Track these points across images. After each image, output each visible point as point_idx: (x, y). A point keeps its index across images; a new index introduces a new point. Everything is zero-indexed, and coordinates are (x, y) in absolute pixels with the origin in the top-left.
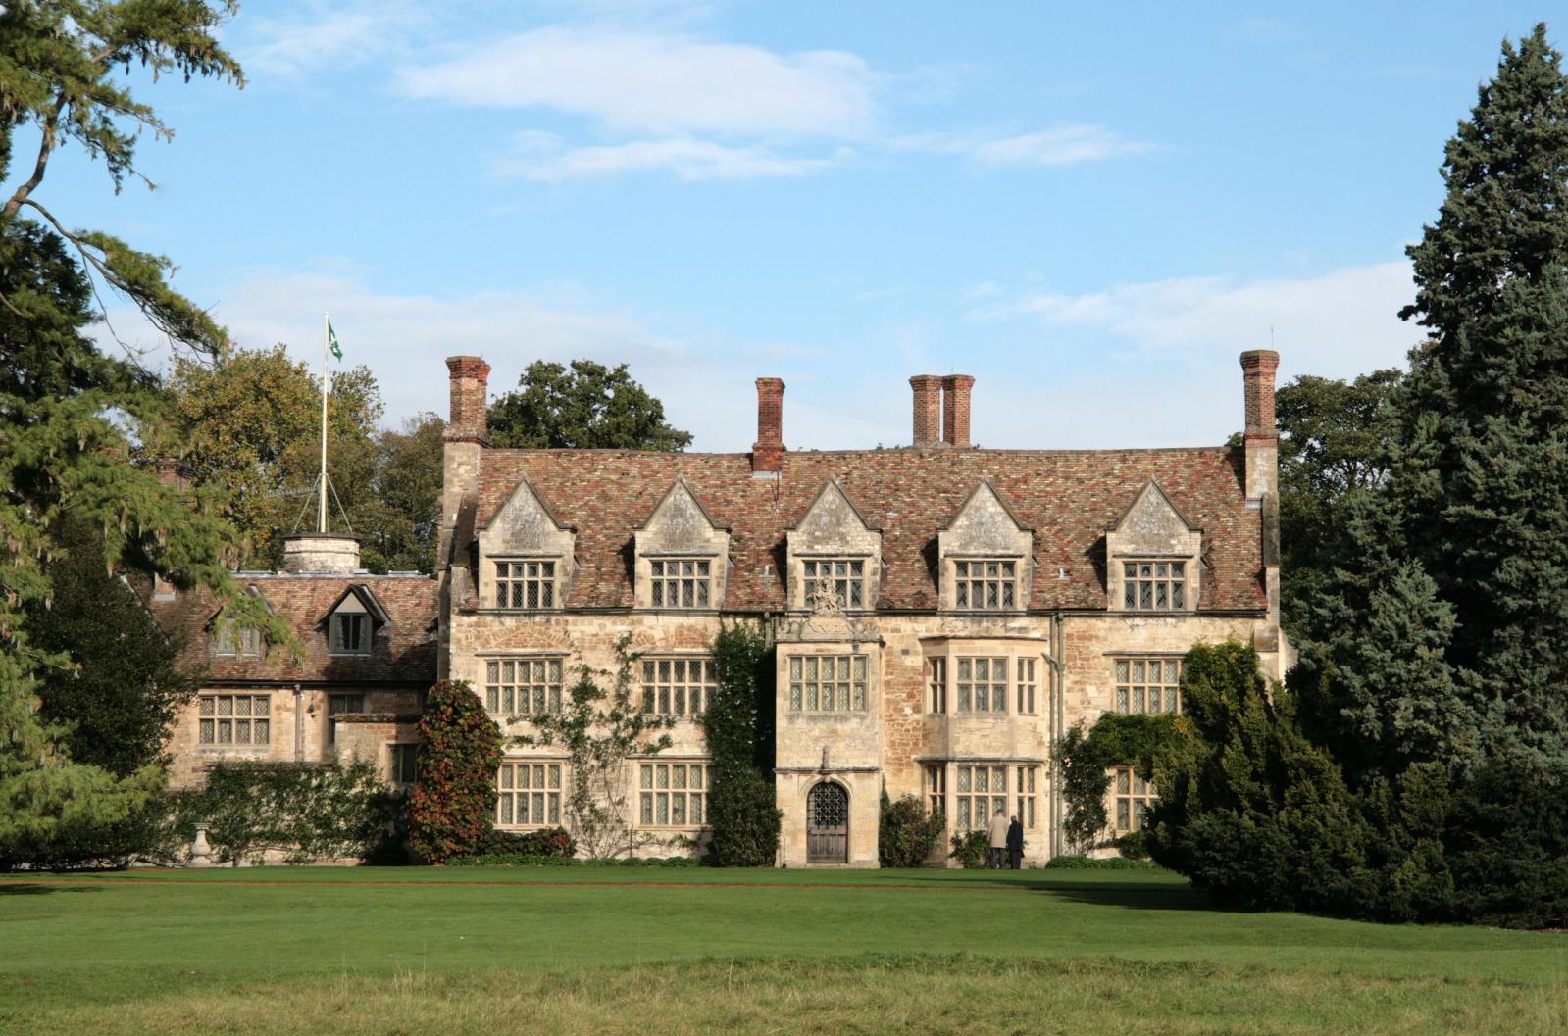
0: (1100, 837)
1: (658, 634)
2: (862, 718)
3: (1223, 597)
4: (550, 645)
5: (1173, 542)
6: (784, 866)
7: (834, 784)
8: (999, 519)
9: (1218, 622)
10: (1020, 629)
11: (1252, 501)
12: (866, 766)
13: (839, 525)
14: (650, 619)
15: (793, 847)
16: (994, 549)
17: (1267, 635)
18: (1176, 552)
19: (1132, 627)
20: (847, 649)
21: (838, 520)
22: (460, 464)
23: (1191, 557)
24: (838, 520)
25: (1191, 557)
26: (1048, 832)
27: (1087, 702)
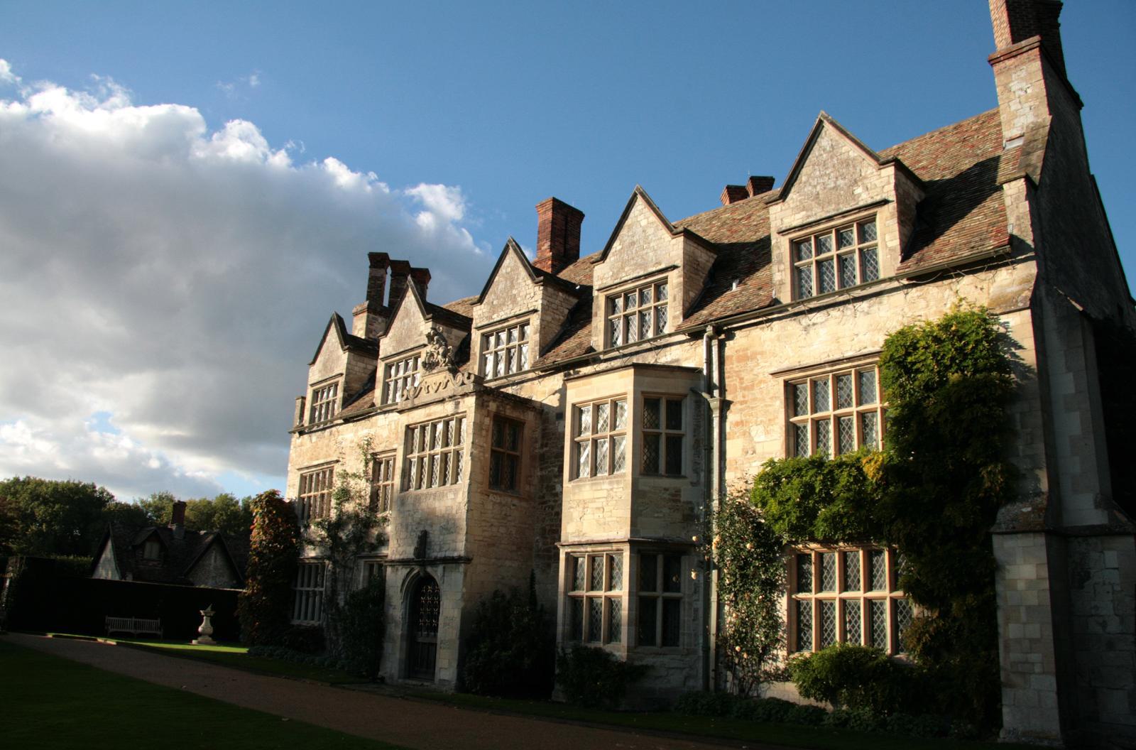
0: (768, 666)
1: (385, 433)
2: (456, 493)
3: (938, 252)
4: (330, 456)
5: (858, 190)
6: (383, 679)
7: (430, 580)
8: (650, 231)
9: (932, 290)
10: (671, 362)
11: (1011, 140)
12: (456, 554)
13: (512, 287)
14: (380, 419)
15: (393, 660)
16: (646, 268)
17: (1015, 288)
18: (861, 204)
19: (806, 329)
20: (449, 408)
21: (512, 283)
22: (359, 330)
23: (885, 202)
24: (512, 283)
25: (885, 202)
26: (701, 653)
27: (750, 451)
